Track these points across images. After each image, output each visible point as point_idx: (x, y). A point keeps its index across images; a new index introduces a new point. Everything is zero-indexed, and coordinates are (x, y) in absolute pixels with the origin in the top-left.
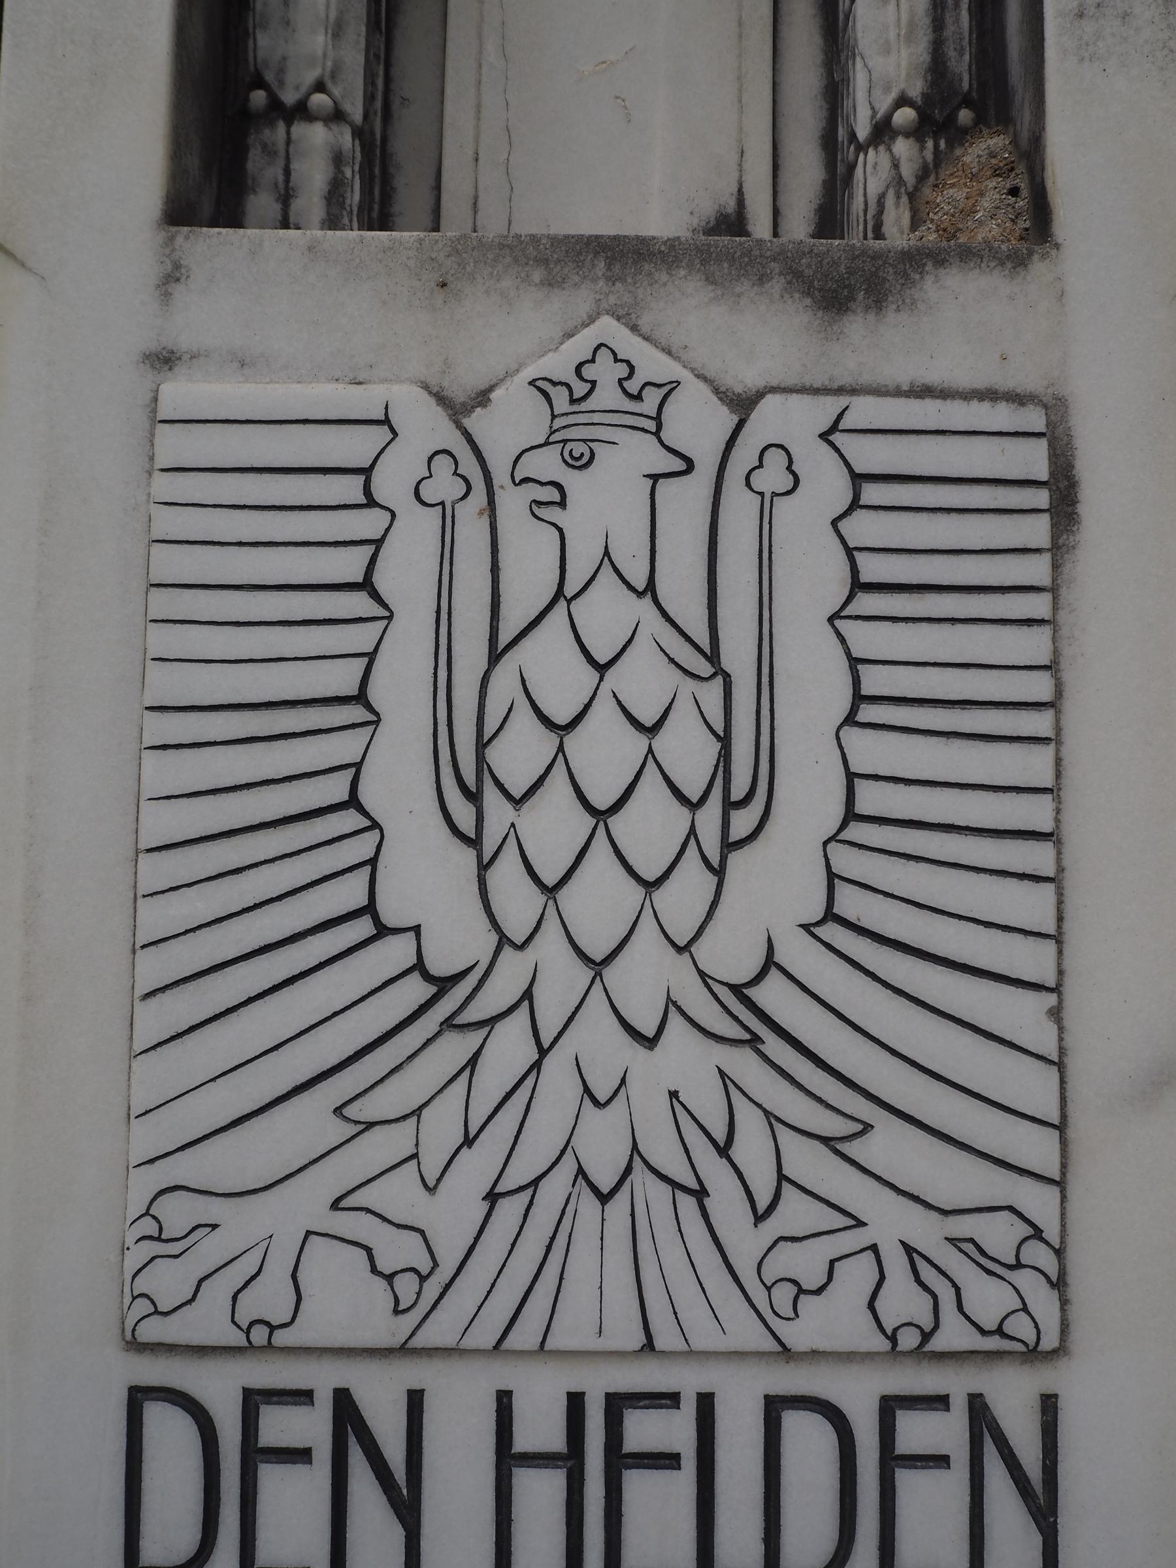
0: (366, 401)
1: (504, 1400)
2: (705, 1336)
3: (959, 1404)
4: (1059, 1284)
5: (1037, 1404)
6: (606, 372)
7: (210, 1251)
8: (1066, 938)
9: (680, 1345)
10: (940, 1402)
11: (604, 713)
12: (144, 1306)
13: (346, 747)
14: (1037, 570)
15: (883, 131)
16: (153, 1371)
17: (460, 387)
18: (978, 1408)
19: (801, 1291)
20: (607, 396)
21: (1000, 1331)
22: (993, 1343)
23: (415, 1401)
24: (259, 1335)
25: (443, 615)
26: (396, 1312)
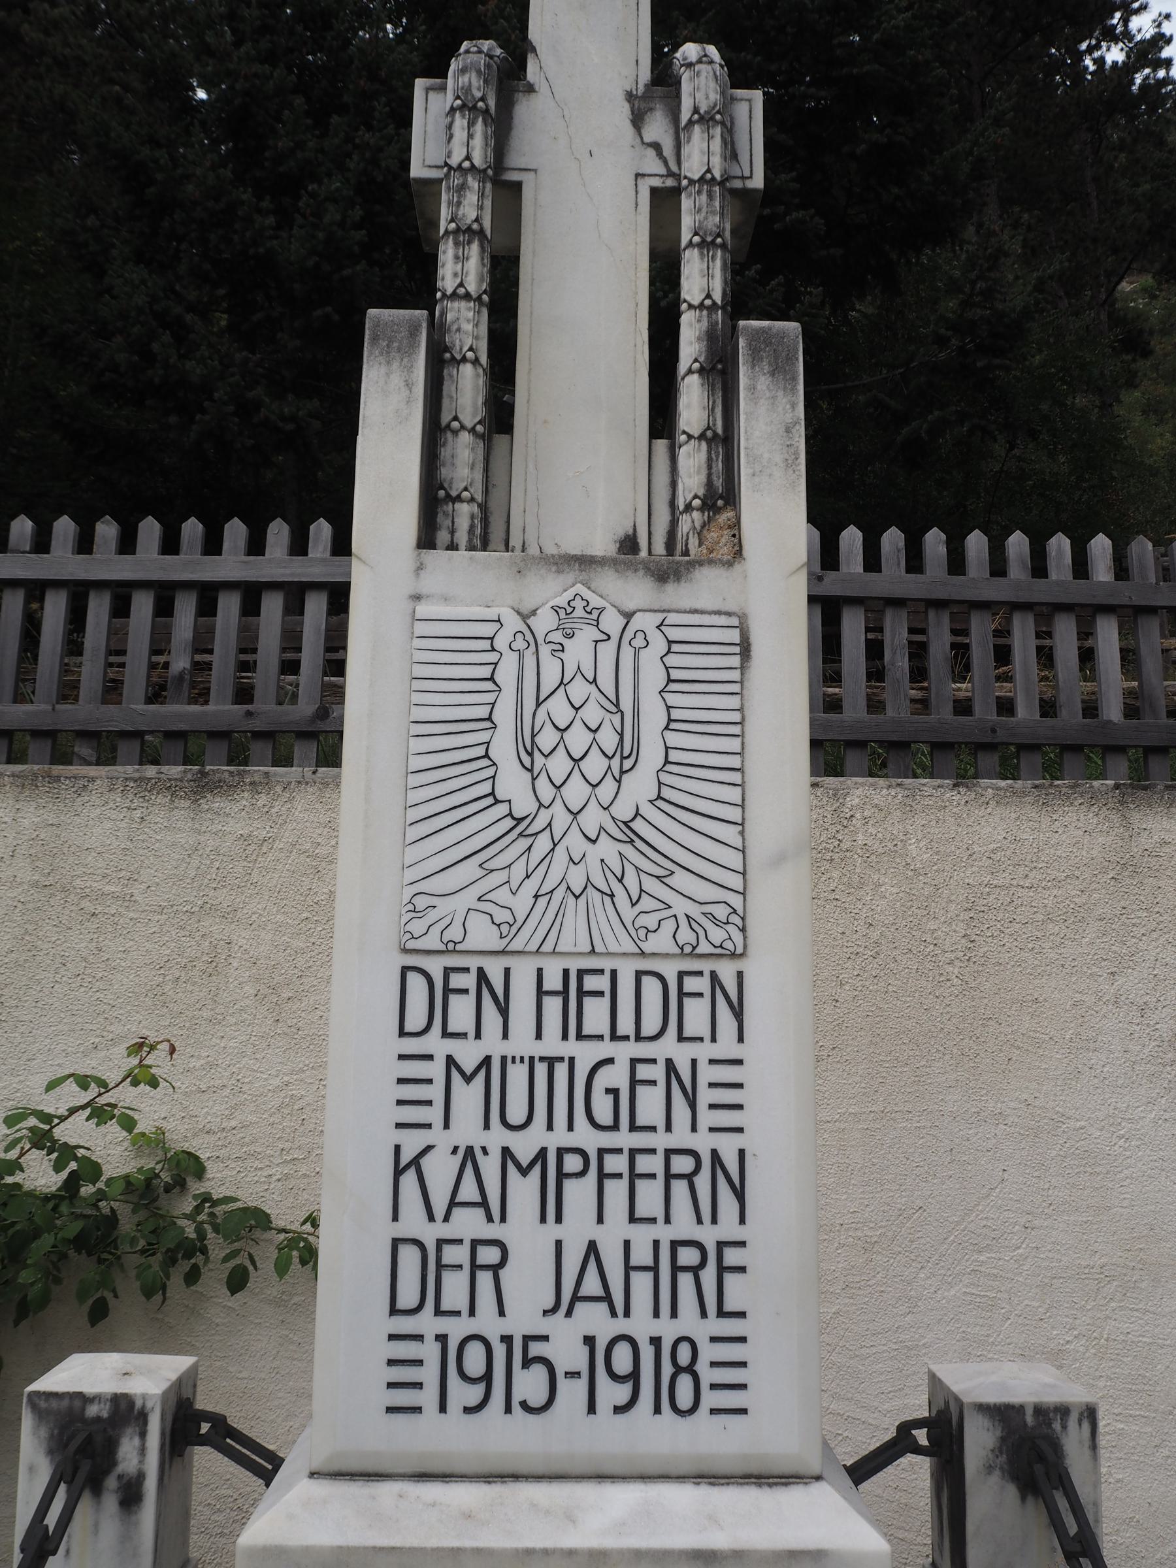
0: (491, 613)
1: (540, 972)
2: (613, 947)
3: (707, 975)
4: (743, 930)
5: (735, 975)
6: (578, 603)
7: (433, 916)
8: (745, 807)
9: (604, 950)
10: (700, 973)
11: (578, 724)
12: (408, 936)
13: (484, 737)
14: (735, 675)
15: (688, 508)
16: (411, 961)
17: (526, 608)
18: (714, 976)
19: (648, 931)
20: (579, 612)
21: (721, 946)
22: (719, 951)
23: (507, 971)
24: (451, 946)
25: (519, 690)
26: (501, 938)
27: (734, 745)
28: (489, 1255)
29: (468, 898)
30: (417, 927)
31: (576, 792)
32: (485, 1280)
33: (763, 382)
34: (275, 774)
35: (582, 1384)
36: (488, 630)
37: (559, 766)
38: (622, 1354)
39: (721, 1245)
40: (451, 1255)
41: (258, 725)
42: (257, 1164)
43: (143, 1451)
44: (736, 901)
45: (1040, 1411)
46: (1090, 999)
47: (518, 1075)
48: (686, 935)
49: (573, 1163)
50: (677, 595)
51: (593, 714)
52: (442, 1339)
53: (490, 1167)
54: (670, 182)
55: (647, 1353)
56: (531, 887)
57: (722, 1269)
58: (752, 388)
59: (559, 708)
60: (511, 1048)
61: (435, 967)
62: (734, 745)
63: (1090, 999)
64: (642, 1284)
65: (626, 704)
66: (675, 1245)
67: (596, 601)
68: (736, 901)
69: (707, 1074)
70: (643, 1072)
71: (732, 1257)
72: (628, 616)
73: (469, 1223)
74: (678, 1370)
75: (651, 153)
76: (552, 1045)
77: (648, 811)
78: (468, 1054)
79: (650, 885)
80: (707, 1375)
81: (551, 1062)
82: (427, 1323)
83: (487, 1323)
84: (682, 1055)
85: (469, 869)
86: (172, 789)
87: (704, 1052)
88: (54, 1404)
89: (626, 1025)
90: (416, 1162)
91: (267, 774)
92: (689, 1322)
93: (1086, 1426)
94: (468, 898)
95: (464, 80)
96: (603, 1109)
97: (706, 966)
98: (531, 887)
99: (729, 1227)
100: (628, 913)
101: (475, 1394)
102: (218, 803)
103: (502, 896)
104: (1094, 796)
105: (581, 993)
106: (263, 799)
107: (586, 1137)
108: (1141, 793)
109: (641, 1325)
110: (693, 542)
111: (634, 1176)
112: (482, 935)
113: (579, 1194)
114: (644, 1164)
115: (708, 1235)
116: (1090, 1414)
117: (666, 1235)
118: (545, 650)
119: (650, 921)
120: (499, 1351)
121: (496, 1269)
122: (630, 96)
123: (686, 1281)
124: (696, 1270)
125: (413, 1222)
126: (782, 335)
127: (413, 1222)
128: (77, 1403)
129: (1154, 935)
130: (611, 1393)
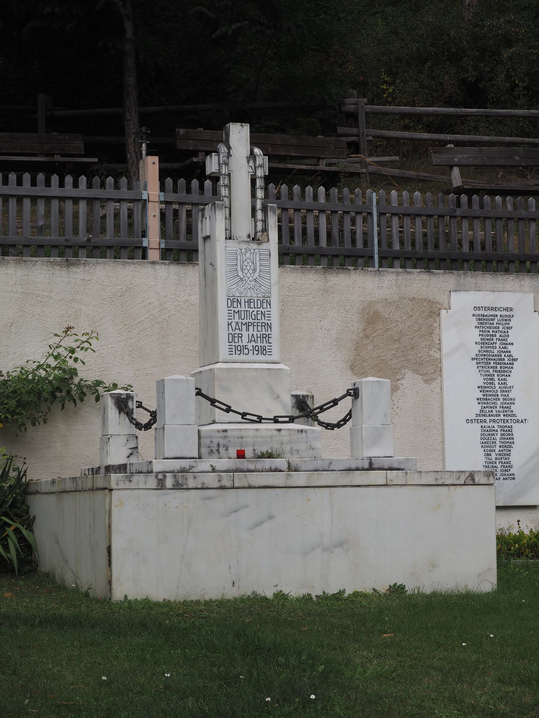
0: (236, 249)
7: (231, 292)
13: (236, 267)
15: (259, 231)
17: (241, 249)
18: (267, 300)
27: (269, 269)
28: (240, 335)
29: (235, 289)
30: (229, 293)
31: (248, 275)
32: (240, 338)
33: (272, 214)
34: (89, 261)
35: (252, 351)
36: (236, 252)
37: (246, 271)
38: (257, 347)
39: (268, 334)
40: (236, 335)
41: (69, 244)
42: (92, 372)
43: (133, 404)
44: (269, 290)
45: (303, 396)
46: (314, 327)
47: (243, 313)
48: (263, 295)
49: (250, 324)
50: (261, 247)
51: (250, 264)
52: (235, 346)
53: (240, 324)
54: (254, 174)
55: (260, 348)
56: (243, 288)
57: (269, 337)
58: (270, 215)
59: (246, 263)
60: (241, 309)
61: (232, 298)
62: (269, 269)
63: (314, 327)
64: (259, 339)
65: (255, 263)
66: (263, 334)
67: (250, 248)
68: (269, 290)
69: (266, 313)
70: (258, 312)
71: (270, 336)
72: (254, 250)
73: (237, 331)
74: (264, 350)
75: (250, 168)
76: (247, 309)
77: (258, 278)
78: (236, 310)
79: (259, 288)
80: (267, 350)
81: (247, 311)
82: (233, 344)
83: (240, 344)
84: (263, 310)
85: (235, 285)
86: (60, 265)
87: (266, 310)
88: (115, 395)
89: (256, 306)
90: (230, 324)
91: (86, 261)
92: (265, 344)
93: (312, 399)
94: (235, 289)
95: (224, 159)
96: (254, 318)
97: (266, 299)
98: (243, 288)
99: (269, 332)
100: (256, 291)
101: (239, 352)
102: (74, 269)
103: (240, 289)
104: (317, 270)
105: (250, 302)
106: (87, 268)
107: (252, 321)
108: (330, 270)
109: (259, 344)
110: (260, 237)
111: (258, 326)
112: (237, 294)
113: (251, 328)
114: (259, 324)
115: (267, 333)
116: (313, 397)
117: (262, 333)
118: (244, 255)
119: (259, 293)
120: (242, 347)
121: (241, 337)
122: (247, 157)
123: (264, 339)
124: (265, 337)
125: (231, 331)
126: (274, 207)
127: (231, 331)
128: (119, 395)
129: (332, 310)
130: (256, 352)
